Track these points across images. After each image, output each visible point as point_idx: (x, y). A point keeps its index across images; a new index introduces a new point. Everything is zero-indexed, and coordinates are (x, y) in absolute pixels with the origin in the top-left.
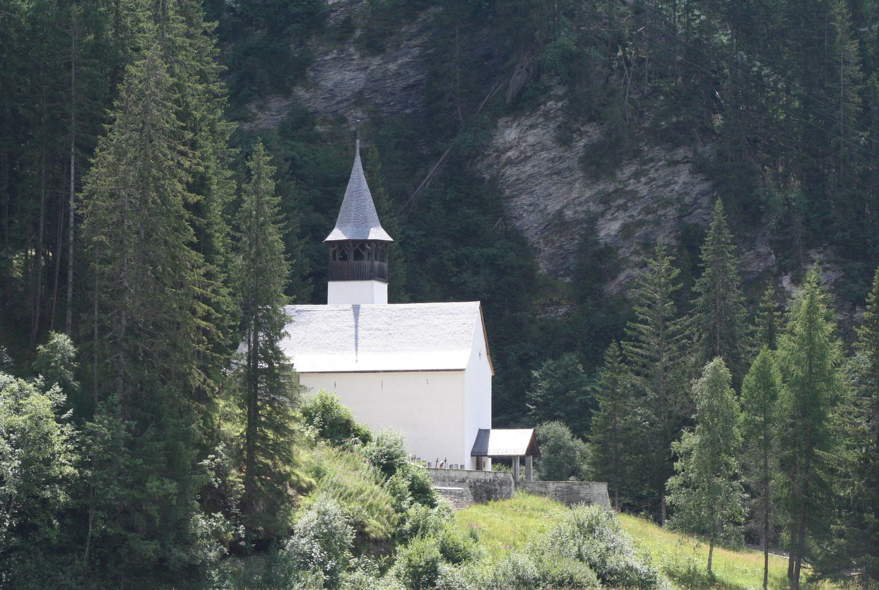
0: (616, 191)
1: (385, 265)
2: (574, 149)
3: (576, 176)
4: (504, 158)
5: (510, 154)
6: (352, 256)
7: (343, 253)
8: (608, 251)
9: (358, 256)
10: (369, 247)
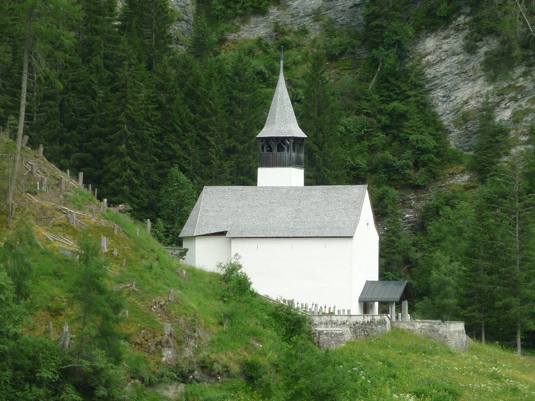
0: (509, 86)
1: (302, 155)
2: (477, 54)
3: (479, 74)
4: (424, 60)
5: (429, 57)
6: (276, 148)
7: (269, 146)
8: (504, 132)
9: (280, 149)
10: (288, 143)
